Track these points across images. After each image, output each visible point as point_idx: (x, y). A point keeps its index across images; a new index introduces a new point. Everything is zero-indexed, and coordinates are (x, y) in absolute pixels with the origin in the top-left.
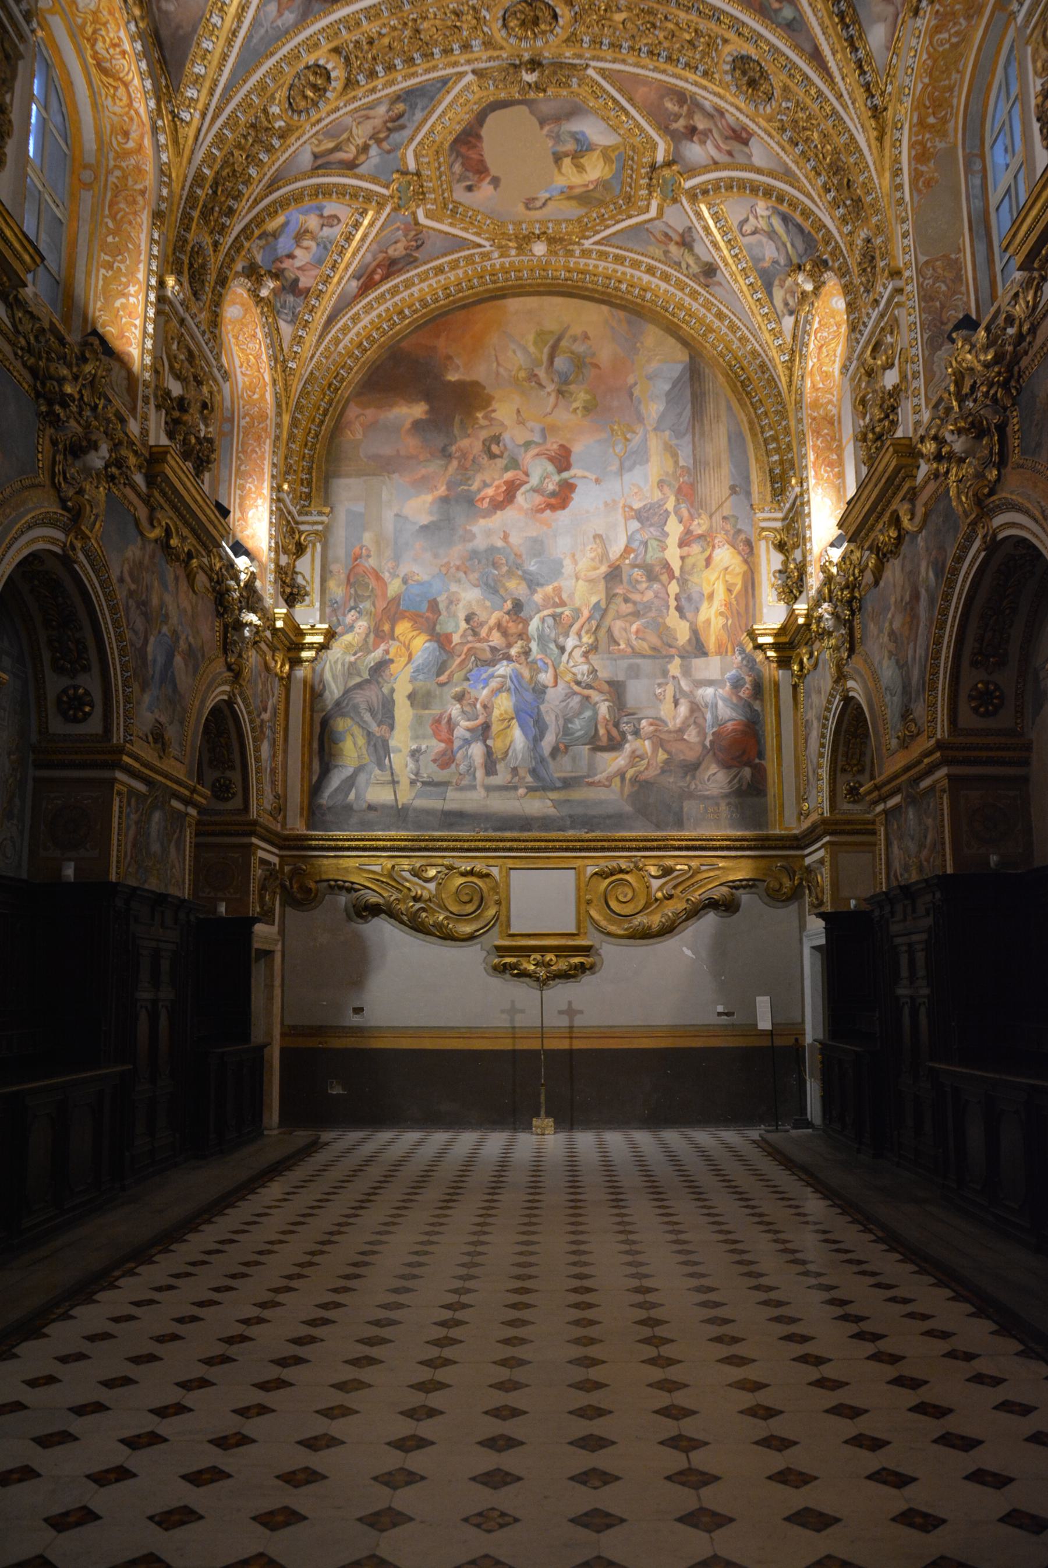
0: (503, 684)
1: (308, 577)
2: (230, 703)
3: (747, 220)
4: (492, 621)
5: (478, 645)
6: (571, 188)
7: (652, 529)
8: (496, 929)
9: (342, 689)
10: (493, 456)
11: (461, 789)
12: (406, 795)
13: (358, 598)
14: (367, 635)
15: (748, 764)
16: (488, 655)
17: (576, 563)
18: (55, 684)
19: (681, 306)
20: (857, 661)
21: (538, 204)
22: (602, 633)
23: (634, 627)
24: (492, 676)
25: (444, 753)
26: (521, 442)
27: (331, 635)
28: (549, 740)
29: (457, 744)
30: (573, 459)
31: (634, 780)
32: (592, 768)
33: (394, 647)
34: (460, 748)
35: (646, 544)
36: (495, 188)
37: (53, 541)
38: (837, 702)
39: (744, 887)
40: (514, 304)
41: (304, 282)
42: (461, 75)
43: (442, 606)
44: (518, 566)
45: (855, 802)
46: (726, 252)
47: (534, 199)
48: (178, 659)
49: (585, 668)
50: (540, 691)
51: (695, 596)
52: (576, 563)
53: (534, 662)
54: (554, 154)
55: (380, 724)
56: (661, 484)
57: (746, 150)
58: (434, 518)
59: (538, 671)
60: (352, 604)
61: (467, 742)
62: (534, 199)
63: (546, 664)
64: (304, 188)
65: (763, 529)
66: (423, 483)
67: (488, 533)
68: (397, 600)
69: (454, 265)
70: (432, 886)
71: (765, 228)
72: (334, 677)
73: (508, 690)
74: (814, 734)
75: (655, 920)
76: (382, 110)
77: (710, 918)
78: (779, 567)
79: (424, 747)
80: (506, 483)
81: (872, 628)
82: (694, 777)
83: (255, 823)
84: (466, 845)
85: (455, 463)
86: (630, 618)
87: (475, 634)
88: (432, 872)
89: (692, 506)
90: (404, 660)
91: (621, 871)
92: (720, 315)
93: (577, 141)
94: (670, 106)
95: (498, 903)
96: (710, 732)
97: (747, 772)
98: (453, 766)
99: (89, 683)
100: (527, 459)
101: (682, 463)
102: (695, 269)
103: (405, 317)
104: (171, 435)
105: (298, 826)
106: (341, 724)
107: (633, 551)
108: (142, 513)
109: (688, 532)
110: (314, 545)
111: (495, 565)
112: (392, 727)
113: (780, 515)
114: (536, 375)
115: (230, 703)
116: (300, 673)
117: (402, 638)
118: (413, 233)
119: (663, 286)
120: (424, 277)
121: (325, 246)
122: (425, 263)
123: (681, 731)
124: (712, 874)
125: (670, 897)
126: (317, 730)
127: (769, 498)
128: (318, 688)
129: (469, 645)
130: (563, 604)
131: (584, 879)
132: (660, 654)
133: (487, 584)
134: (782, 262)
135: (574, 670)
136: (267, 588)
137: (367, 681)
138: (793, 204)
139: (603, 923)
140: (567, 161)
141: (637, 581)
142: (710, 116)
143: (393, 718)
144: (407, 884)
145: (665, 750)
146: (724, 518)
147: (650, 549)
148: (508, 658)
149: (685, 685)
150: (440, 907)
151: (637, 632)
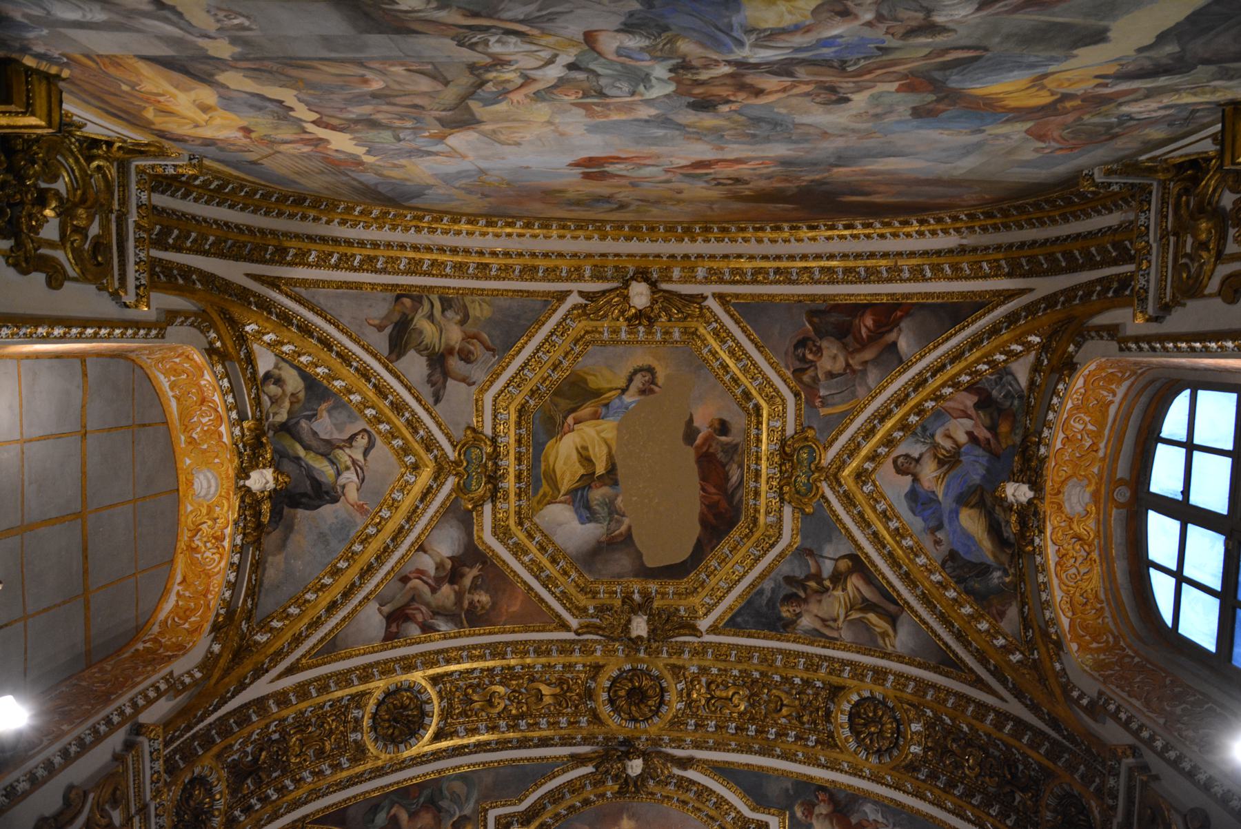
3: (366, 453)
6: (596, 416)
21: (639, 381)
36: (691, 420)
41: (969, 400)
42: (713, 629)
54: (615, 483)
57: (386, 609)
62: (642, 392)
71: (339, 452)
76: (806, 622)
93: (588, 507)
118: (806, 378)
121: (923, 432)
122: (800, 300)
134: (304, 423)
140: (600, 469)
142: (437, 612)
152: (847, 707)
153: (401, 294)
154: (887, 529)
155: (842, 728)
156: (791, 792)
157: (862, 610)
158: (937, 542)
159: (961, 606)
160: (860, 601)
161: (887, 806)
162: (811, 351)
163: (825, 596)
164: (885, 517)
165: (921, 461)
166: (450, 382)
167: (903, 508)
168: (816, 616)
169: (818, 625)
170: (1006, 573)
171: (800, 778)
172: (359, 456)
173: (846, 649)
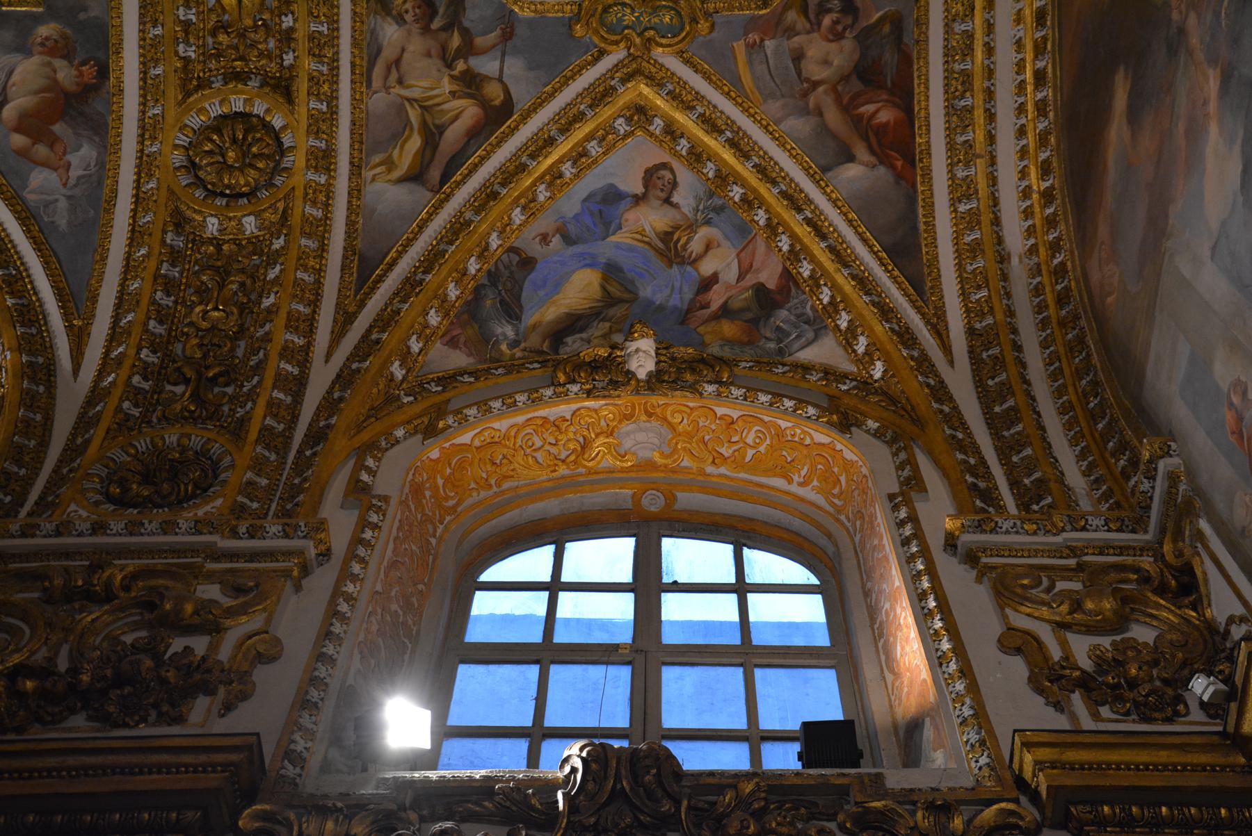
41: (769, 276)
76: (390, 33)
152: (259, 108)
154: (561, 161)
155: (221, 103)
156: (82, 16)
157: (424, 125)
158: (545, 239)
159: (458, 282)
160: (437, 122)
161: (100, 183)
162: (836, 22)
163: (439, 63)
164: (579, 155)
165: (667, 207)
167: (592, 182)
168: (403, 50)
169: (388, 54)
170: (514, 344)
171: (113, 31)
173: (356, 103)
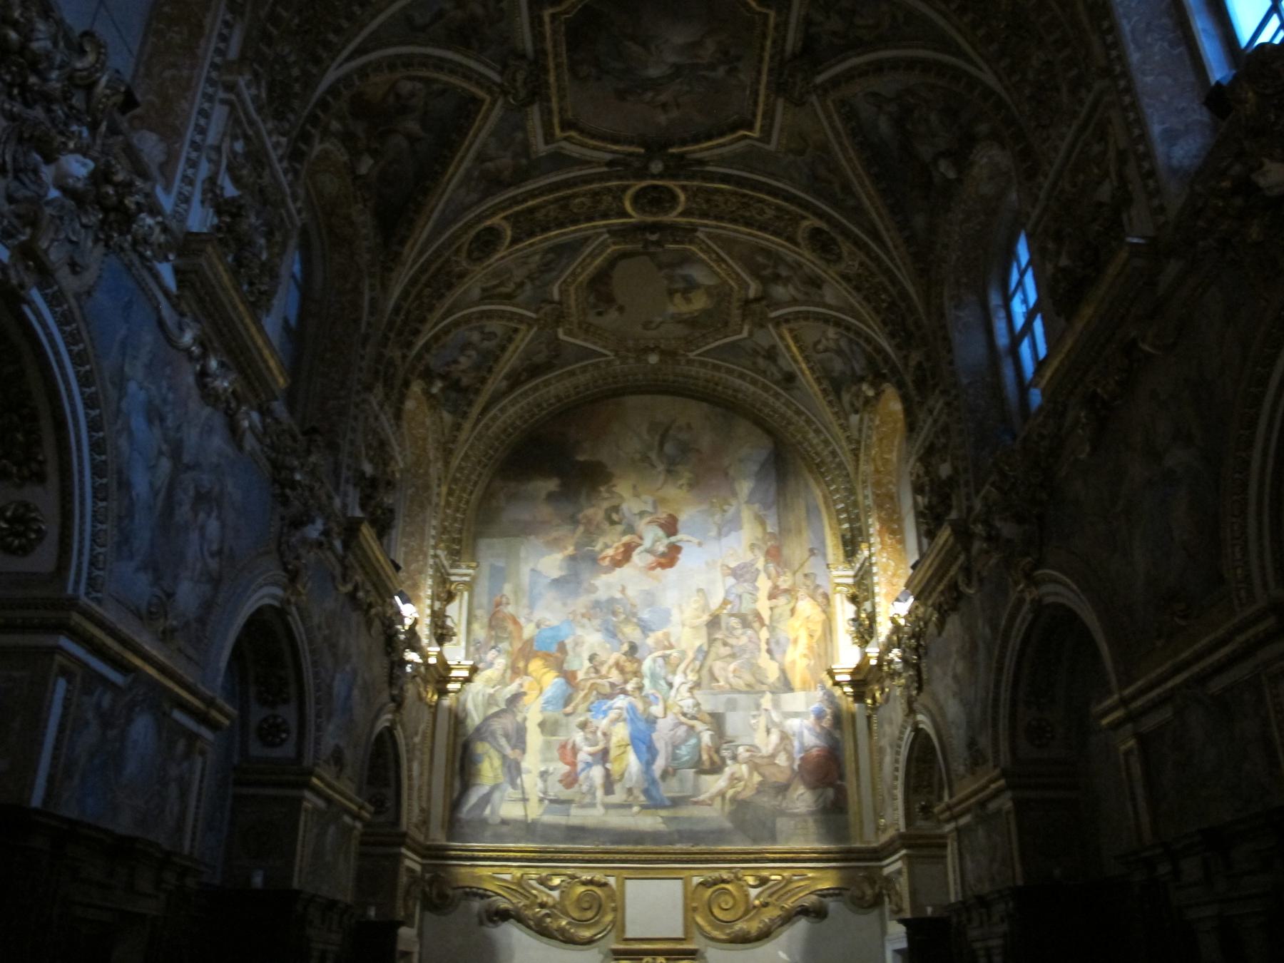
0: (620, 715)
1: (456, 621)
2: (390, 730)
4: (612, 661)
5: (599, 681)
6: (680, 314)
7: (745, 584)
8: (612, 935)
9: (482, 718)
10: (613, 523)
11: (583, 806)
12: (535, 812)
13: (498, 639)
14: (505, 671)
15: (831, 785)
16: (608, 690)
17: (682, 612)
18: (258, 714)
19: (765, 404)
20: (924, 698)
21: (653, 325)
22: (705, 672)
23: (732, 667)
24: (610, 708)
25: (568, 775)
26: (636, 511)
27: (474, 670)
28: (659, 764)
29: (580, 766)
30: (680, 525)
31: (734, 800)
32: (697, 789)
33: (527, 681)
34: (583, 770)
35: (740, 597)
37: (274, 597)
38: (908, 734)
39: (831, 895)
40: (631, 401)
41: (465, 381)
43: (569, 647)
44: (634, 615)
45: (926, 819)
46: (804, 366)
47: (651, 322)
48: (356, 692)
49: (690, 702)
50: (652, 721)
51: (782, 641)
52: (682, 612)
53: (647, 696)
55: (514, 747)
56: (752, 547)
58: (563, 573)
59: (650, 704)
60: (493, 643)
61: (589, 765)
62: (651, 322)
63: (657, 698)
64: (473, 313)
65: (838, 585)
66: (555, 544)
67: (609, 586)
68: (530, 641)
69: (584, 370)
70: (556, 894)
72: (476, 706)
73: (625, 720)
74: (888, 759)
75: (753, 926)
76: (537, 257)
77: (802, 925)
78: (853, 616)
79: (551, 769)
80: (624, 545)
81: (937, 670)
82: (784, 798)
83: (405, 835)
84: (587, 857)
85: (581, 529)
86: (729, 659)
87: (597, 671)
88: (556, 881)
89: (778, 564)
90: (536, 693)
91: (724, 881)
92: (798, 412)
94: (760, 259)
95: (615, 910)
96: (798, 756)
97: (830, 792)
98: (576, 786)
99: (288, 713)
100: (641, 525)
101: (769, 530)
102: (778, 376)
103: (543, 409)
104: (363, 507)
105: (439, 838)
106: (481, 748)
107: (730, 602)
108: (338, 571)
109: (776, 587)
110: (462, 594)
111: (614, 613)
112: (524, 751)
113: (851, 573)
114: (648, 458)
115: (390, 730)
116: (447, 701)
117: (534, 674)
119: (752, 388)
120: (560, 378)
123: (773, 756)
124: (802, 883)
125: (765, 905)
126: (459, 752)
127: (841, 558)
128: (461, 715)
129: (592, 681)
130: (671, 647)
131: (691, 889)
132: (754, 689)
133: (607, 630)
135: (681, 703)
136: (424, 631)
137: (503, 711)
138: (858, 333)
139: (708, 928)
141: (734, 628)
143: (524, 742)
144: (534, 892)
145: (760, 774)
146: (806, 575)
147: (744, 601)
148: (624, 692)
149: (775, 716)
150: (563, 913)
151: (734, 671)
153: (786, 389)
166: (767, 347)
172: (824, 341)
